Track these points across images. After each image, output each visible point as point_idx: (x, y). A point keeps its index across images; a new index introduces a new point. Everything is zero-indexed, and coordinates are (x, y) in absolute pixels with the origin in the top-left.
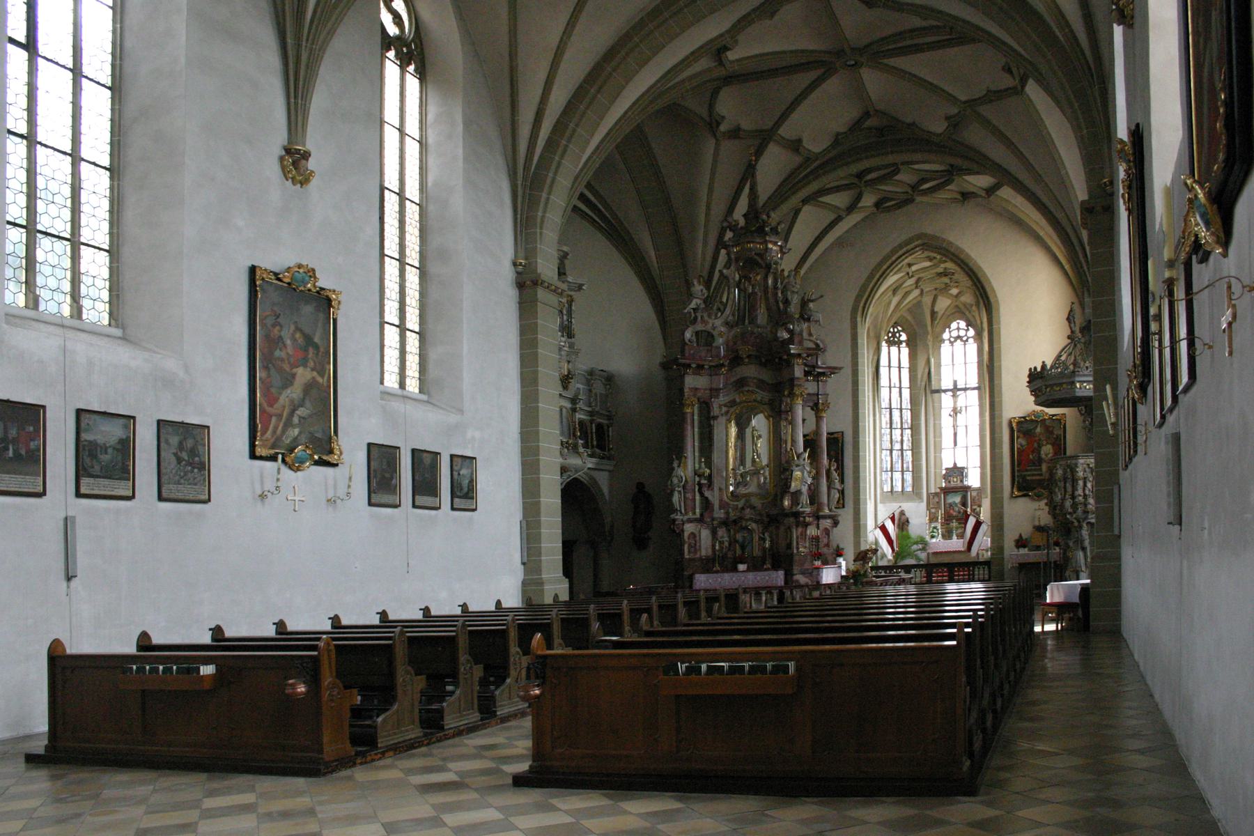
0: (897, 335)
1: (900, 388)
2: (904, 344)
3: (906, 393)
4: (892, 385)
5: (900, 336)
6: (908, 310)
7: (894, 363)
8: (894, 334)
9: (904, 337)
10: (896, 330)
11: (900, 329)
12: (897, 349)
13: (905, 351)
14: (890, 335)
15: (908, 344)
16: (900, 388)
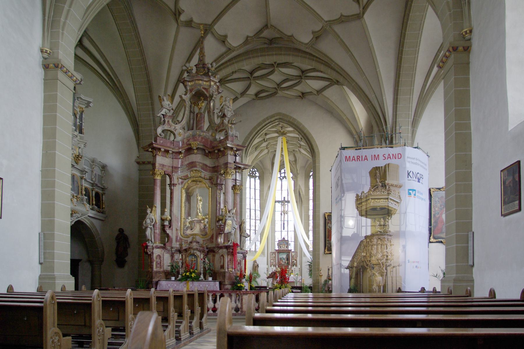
0: (254, 173)
1: (255, 199)
2: (257, 178)
3: (258, 202)
4: (251, 198)
5: (256, 173)
6: (260, 161)
7: (253, 186)
8: (253, 173)
9: (257, 174)
10: (254, 170)
11: (256, 170)
12: (254, 180)
13: (258, 181)
14: (251, 172)
15: (260, 177)
16: (255, 199)
